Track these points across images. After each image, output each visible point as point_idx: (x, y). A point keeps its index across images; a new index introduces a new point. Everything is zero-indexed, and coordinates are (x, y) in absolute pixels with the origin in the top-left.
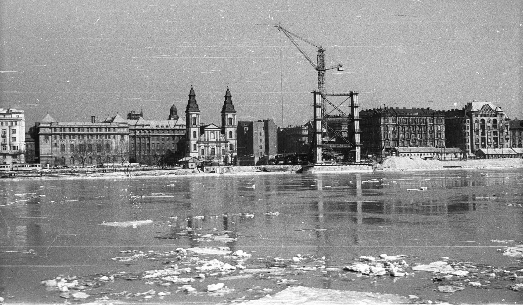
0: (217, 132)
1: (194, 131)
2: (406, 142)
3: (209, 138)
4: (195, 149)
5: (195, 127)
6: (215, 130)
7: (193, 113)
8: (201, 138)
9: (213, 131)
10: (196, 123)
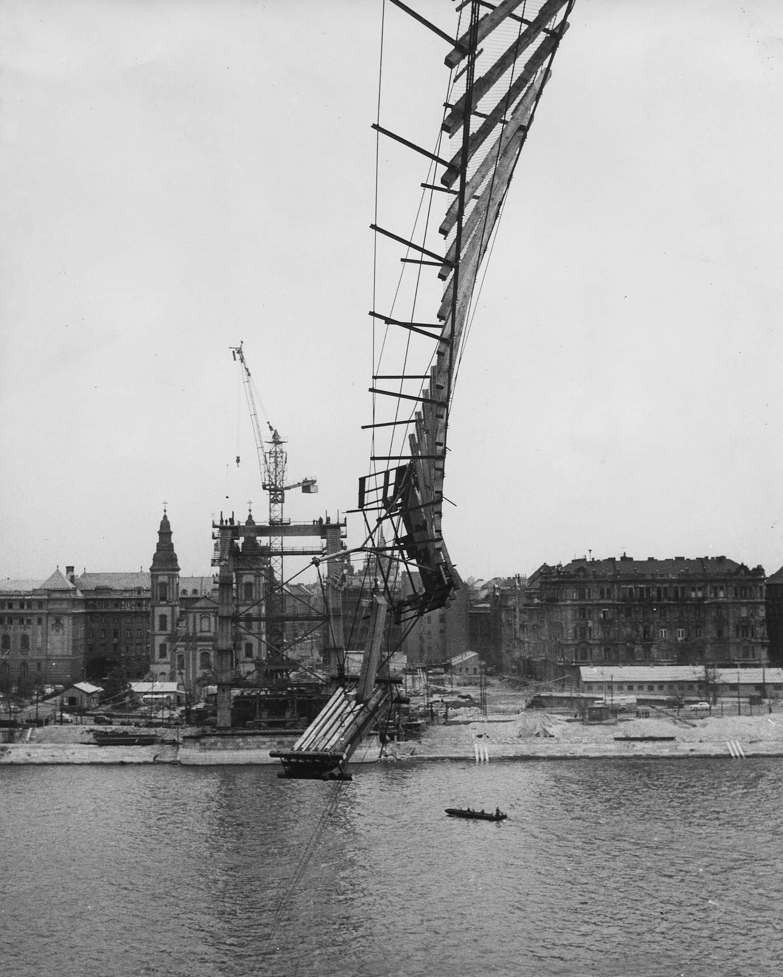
2: (638, 649)
4: (163, 655)
5: (164, 606)
7: (162, 573)
8: (178, 630)
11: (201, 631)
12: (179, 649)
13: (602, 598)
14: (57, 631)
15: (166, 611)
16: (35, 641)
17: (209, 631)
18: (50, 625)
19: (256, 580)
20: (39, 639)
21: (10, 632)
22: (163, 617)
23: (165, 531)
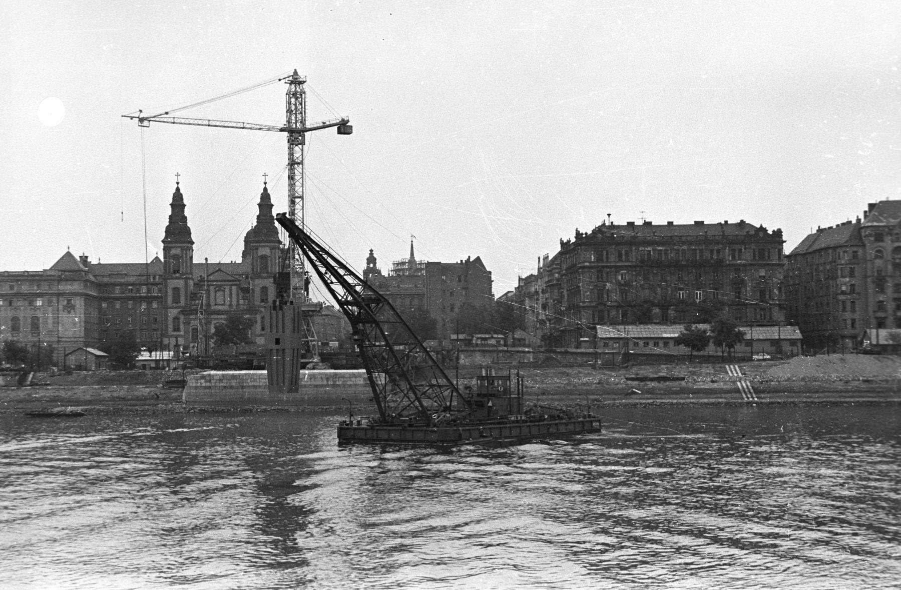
0: (231, 290)
1: (173, 286)
3: (212, 302)
5: (177, 278)
6: (227, 285)
7: (174, 245)
9: (221, 286)
10: (179, 267)
11: (216, 305)
12: (193, 323)
13: (620, 260)
14: (69, 312)
15: (180, 283)
16: (46, 323)
17: (224, 304)
18: (61, 307)
19: (271, 252)
20: (50, 321)
21: (20, 314)
22: (176, 290)
23: (178, 203)
